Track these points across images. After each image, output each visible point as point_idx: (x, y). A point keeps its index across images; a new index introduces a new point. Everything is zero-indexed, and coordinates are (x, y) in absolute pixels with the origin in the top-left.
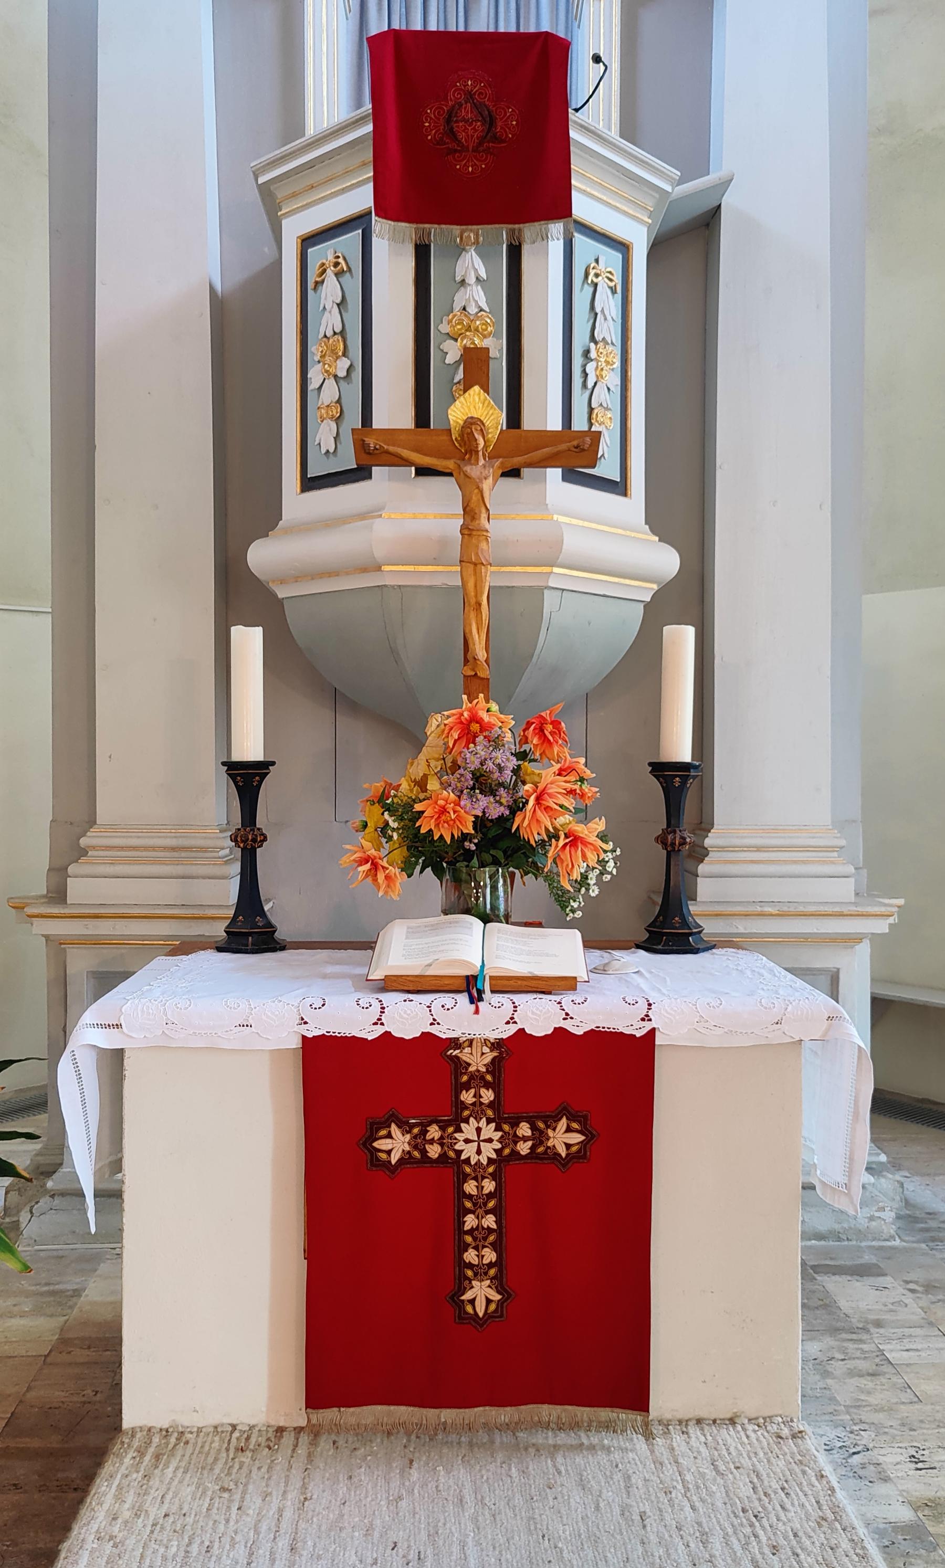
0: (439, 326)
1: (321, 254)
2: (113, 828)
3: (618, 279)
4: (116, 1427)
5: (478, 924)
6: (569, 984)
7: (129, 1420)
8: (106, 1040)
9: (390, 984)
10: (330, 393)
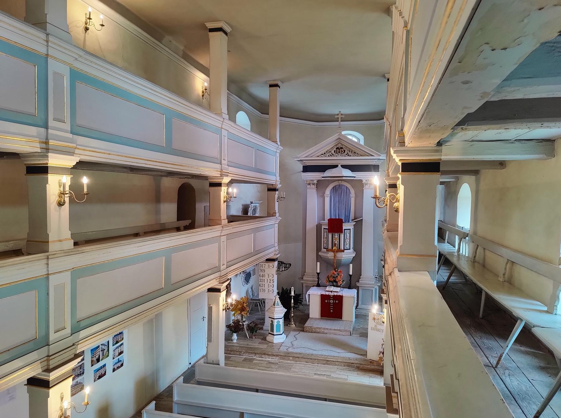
0: (334, 239)
1: (325, 230)
4: (309, 317)
6: (338, 292)
7: (310, 317)
8: (309, 293)
9: (326, 291)
10: (325, 242)
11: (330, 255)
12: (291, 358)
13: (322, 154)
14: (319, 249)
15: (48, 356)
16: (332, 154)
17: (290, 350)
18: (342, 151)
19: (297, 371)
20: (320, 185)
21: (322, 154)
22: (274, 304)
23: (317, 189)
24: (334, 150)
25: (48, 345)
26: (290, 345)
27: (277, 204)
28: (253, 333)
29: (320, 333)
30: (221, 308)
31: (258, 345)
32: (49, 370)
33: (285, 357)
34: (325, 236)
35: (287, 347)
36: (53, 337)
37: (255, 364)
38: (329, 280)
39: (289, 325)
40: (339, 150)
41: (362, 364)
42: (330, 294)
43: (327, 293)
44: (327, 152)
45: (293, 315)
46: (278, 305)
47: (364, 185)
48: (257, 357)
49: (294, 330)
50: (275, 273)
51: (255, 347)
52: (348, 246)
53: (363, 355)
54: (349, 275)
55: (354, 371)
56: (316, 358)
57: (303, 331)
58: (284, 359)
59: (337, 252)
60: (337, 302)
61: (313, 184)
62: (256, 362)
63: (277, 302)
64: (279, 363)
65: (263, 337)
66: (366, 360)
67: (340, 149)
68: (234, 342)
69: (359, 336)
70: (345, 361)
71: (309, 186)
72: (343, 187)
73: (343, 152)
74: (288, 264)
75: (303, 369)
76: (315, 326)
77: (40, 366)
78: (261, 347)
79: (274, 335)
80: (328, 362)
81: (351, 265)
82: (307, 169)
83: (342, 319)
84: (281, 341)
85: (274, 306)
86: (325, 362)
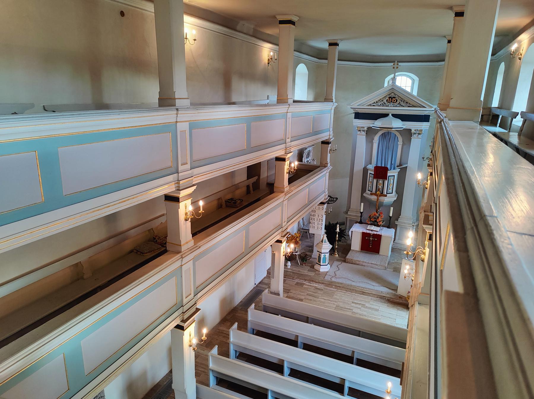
0: (378, 183)
1: (371, 175)
2: (351, 209)
3: (393, 179)
4: (350, 249)
5: (374, 226)
6: (378, 231)
8: (352, 230)
9: (367, 230)
11: (374, 198)
12: (334, 287)
13: (375, 103)
14: (363, 190)
15: (183, 313)
16: (384, 103)
17: (333, 280)
18: (394, 101)
19: (338, 298)
20: (370, 132)
21: (375, 103)
22: (322, 241)
23: (366, 136)
24: (386, 99)
25: (182, 306)
26: (333, 274)
27: (329, 155)
28: (303, 262)
29: (359, 265)
30: (282, 254)
31: (307, 272)
32: (184, 321)
33: (329, 285)
34: (371, 180)
35: (331, 277)
36: (185, 301)
37: (305, 288)
38: (370, 220)
39: (333, 255)
40: (391, 99)
41: (392, 298)
42: (370, 232)
43: (368, 232)
44: (379, 101)
45: (337, 247)
46: (325, 242)
47: (413, 134)
48: (306, 282)
49: (338, 260)
50: (324, 214)
51: (305, 274)
52: (390, 191)
53: (394, 290)
54: (389, 216)
55: (385, 303)
56: (354, 289)
57: (345, 261)
58: (328, 287)
59: (380, 196)
60: (376, 239)
61: (364, 131)
62: (306, 286)
63: (325, 239)
64: (324, 290)
65: (311, 265)
66: (396, 295)
67: (392, 99)
68: (288, 267)
69: (392, 270)
70: (378, 294)
71: (359, 133)
72: (392, 135)
73: (396, 101)
74: (335, 198)
75: (343, 297)
76: (355, 259)
77: (179, 319)
78: (310, 274)
79: (321, 265)
80: (364, 293)
81: (392, 208)
82: (358, 116)
83: (379, 253)
84: (327, 270)
85: (322, 243)
86: (361, 293)
